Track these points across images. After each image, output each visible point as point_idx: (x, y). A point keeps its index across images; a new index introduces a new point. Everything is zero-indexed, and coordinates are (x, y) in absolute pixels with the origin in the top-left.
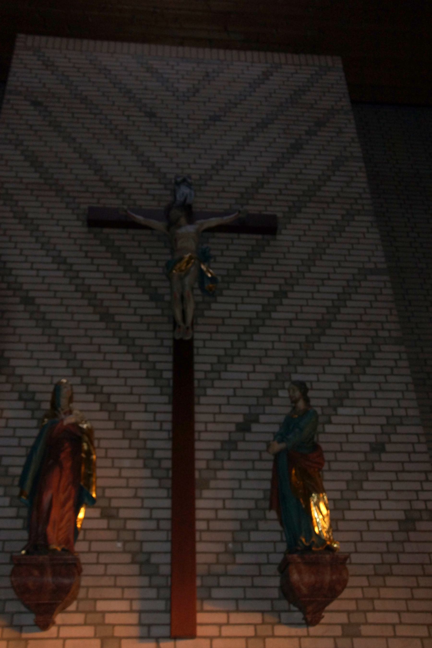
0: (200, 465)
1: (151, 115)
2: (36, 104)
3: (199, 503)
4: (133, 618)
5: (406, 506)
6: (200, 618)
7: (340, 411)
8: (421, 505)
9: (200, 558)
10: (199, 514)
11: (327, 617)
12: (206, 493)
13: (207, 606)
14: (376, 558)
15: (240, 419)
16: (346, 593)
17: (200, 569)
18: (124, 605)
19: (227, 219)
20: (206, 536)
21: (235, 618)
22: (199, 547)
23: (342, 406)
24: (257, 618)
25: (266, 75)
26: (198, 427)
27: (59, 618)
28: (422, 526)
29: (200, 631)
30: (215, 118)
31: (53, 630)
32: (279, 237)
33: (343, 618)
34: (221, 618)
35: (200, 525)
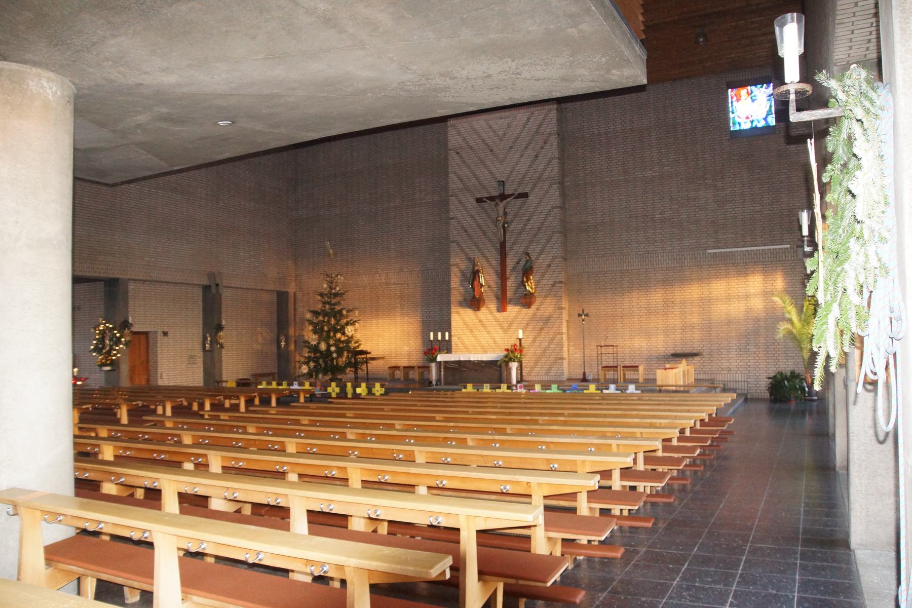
1: (491, 151)
2: (458, 153)
3: (508, 283)
4: (495, 308)
7: (542, 256)
8: (557, 280)
10: (508, 285)
11: (532, 307)
14: (545, 294)
15: (517, 260)
17: (508, 298)
18: (493, 306)
21: (515, 307)
22: (508, 293)
24: (519, 307)
25: (529, 119)
26: (507, 264)
28: (557, 285)
30: (511, 148)
31: (481, 311)
32: (529, 198)
33: (536, 307)
34: (512, 308)
35: (508, 288)
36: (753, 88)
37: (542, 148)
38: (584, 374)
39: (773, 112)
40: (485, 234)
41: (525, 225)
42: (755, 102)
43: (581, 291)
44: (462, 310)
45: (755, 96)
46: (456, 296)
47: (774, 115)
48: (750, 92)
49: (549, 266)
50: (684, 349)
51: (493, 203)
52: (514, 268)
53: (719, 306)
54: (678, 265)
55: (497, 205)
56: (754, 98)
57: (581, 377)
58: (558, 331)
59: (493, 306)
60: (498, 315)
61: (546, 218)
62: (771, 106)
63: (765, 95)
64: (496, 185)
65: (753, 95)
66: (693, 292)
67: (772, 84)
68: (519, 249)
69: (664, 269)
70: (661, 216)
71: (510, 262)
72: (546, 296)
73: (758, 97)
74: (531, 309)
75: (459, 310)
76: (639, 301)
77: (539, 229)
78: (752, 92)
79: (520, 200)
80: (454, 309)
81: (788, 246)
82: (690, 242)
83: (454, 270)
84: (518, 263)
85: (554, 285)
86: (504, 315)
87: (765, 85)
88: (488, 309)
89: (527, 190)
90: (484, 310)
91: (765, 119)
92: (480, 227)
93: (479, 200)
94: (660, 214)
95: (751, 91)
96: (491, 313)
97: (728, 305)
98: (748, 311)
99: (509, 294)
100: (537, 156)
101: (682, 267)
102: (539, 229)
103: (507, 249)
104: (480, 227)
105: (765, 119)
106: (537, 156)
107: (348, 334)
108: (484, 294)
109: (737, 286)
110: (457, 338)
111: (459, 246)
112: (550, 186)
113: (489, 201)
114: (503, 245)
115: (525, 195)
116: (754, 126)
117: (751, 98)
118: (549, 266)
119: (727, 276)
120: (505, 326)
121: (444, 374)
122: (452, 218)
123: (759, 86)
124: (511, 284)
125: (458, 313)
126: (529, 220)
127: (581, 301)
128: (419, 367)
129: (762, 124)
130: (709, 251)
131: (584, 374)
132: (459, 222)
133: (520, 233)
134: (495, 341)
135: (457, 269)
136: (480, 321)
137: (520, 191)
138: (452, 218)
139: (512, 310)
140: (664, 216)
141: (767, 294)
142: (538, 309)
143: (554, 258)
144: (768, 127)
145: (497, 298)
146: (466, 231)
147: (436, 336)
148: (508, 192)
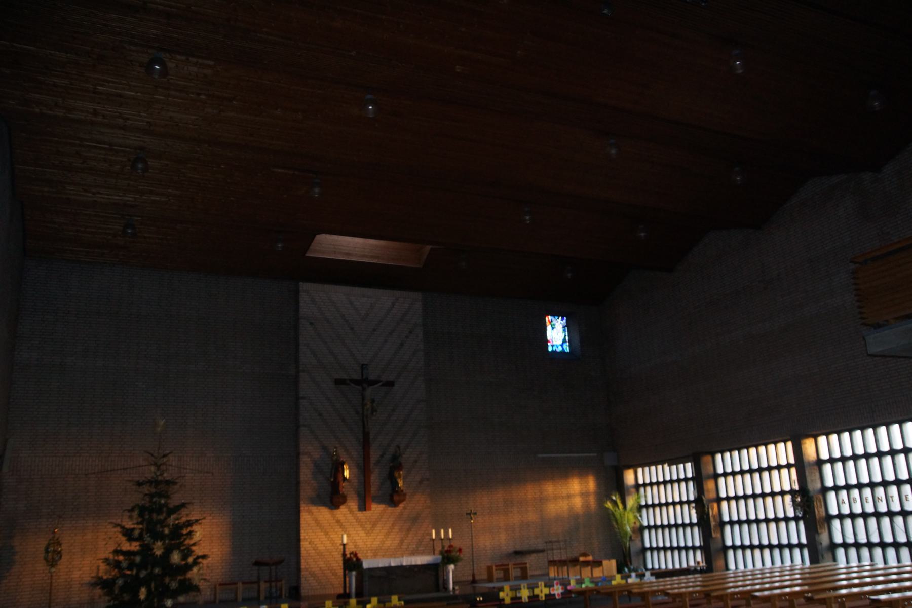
1: (352, 329)
2: (311, 324)
18: (354, 504)
24: (384, 506)
25: (393, 304)
29: (373, 509)
30: (374, 330)
36: (553, 318)
37: (407, 337)
38: (473, 575)
39: (567, 341)
42: (554, 329)
44: (315, 508)
45: (554, 325)
46: (307, 490)
47: (568, 344)
48: (550, 321)
49: (416, 461)
51: (359, 387)
55: (364, 389)
56: (553, 326)
57: (470, 578)
59: (353, 504)
60: (360, 515)
62: (565, 336)
63: (561, 326)
65: (552, 323)
66: (530, 491)
67: (565, 318)
71: (374, 455)
73: (556, 326)
74: (397, 508)
75: (310, 508)
78: (552, 321)
80: (303, 507)
81: (595, 455)
83: (305, 459)
84: (382, 456)
85: (421, 482)
87: (560, 317)
88: (349, 508)
89: (391, 378)
90: (343, 509)
91: (562, 345)
93: (339, 382)
95: (551, 320)
96: (351, 511)
98: (571, 509)
99: (373, 490)
100: (402, 344)
105: (562, 345)
106: (402, 344)
110: (307, 543)
113: (353, 385)
114: (366, 435)
115: (390, 384)
116: (554, 350)
117: (551, 325)
118: (416, 461)
122: (303, 398)
123: (556, 318)
124: (375, 478)
125: (310, 512)
128: (220, 584)
129: (560, 349)
131: (473, 575)
135: (309, 459)
136: (338, 521)
137: (384, 378)
138: (303, 398)
139: (377, 509)
141: (584, 495)
142: (405, 508)
144: (563, 352)
145: (359, 495)
146: (320, 415)
147: (438, 533)
148: (372, 377)
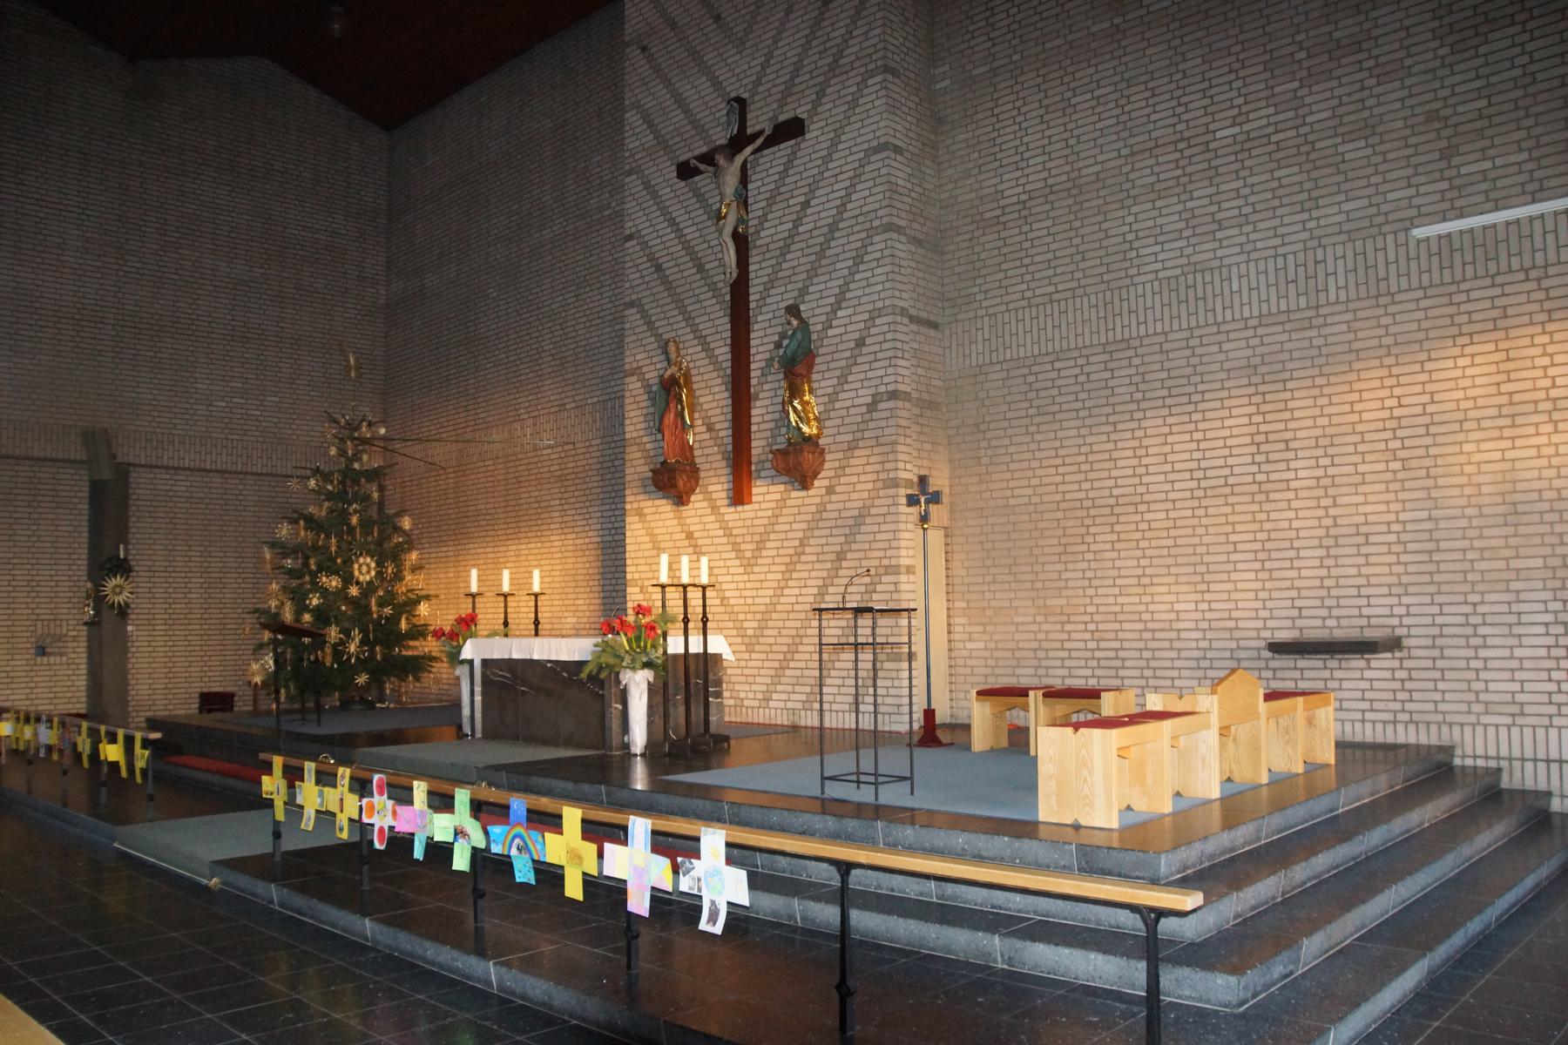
0: (754, 382)
3: (754, 412)
5: (872, 391)
6: (754, 491)
8: (882, 389)
9: (754, 452)
10: (753, 420)
11: (817, 483)
12: (758, 403)
13: (758, 483)
16: (827, 465)
17: (754, 459)
19: (760, 141)
20: (758, 435)
21: (772, 489)
22: (754, 444)
23: (840, 309)
24: (782, 488)
27: (693, 498)
28: (882, 406)
29: (754, 499)
32: (808, 136)
33: (826, 483)
34: (764, 489)
35: (754, 428)
40: (700, 268)
41: (797, 223)
43: (983, 427)
44: (649, 503)
49: (860, 343)
50: (1331, 623)
52: (769, 362)
53: (1467, 448)
54: (1303, 304)
58: (885, 562)
61: (851, 190)
64: (722, 110)
68: (781, 297)
69: (1254, 322)
70: (1237, 129)
72: (852, 446)
74: (811, 492)
75: (642, 504)
76: (1167, 449)
77: (833, 228)
79: (786, 147)
82: (1345, 207)
83: (634, 386)
85: (872, 407)
86: (743, 515)
90: (697, 501)
92: (687, 247)
94: (1234, 125)
97: (1507, 444)
99: (758, 446)
101: (1317, 307)
102: (833, 228)
103: (753, 305)
104: (687, 247)
107: (361, 578)
108: (696, 453)
109: (1546, 361)
110: (638, 589)
111: (644, 314)
112: (863, 84)
118: (860, 343)
119: (1500, 322)
120: (748, 548)
121: (483, 701)
125: (640, 513)
126: (806, 205)
127: (985, 461)
130: (1419, 233)
131: (929, 714)
132: (644, 245)
133: (785, 250)
134: (723, 599)
139: (767, 493)
140: (1246, 128)
142: (830, 490)
143: (874, 314)
